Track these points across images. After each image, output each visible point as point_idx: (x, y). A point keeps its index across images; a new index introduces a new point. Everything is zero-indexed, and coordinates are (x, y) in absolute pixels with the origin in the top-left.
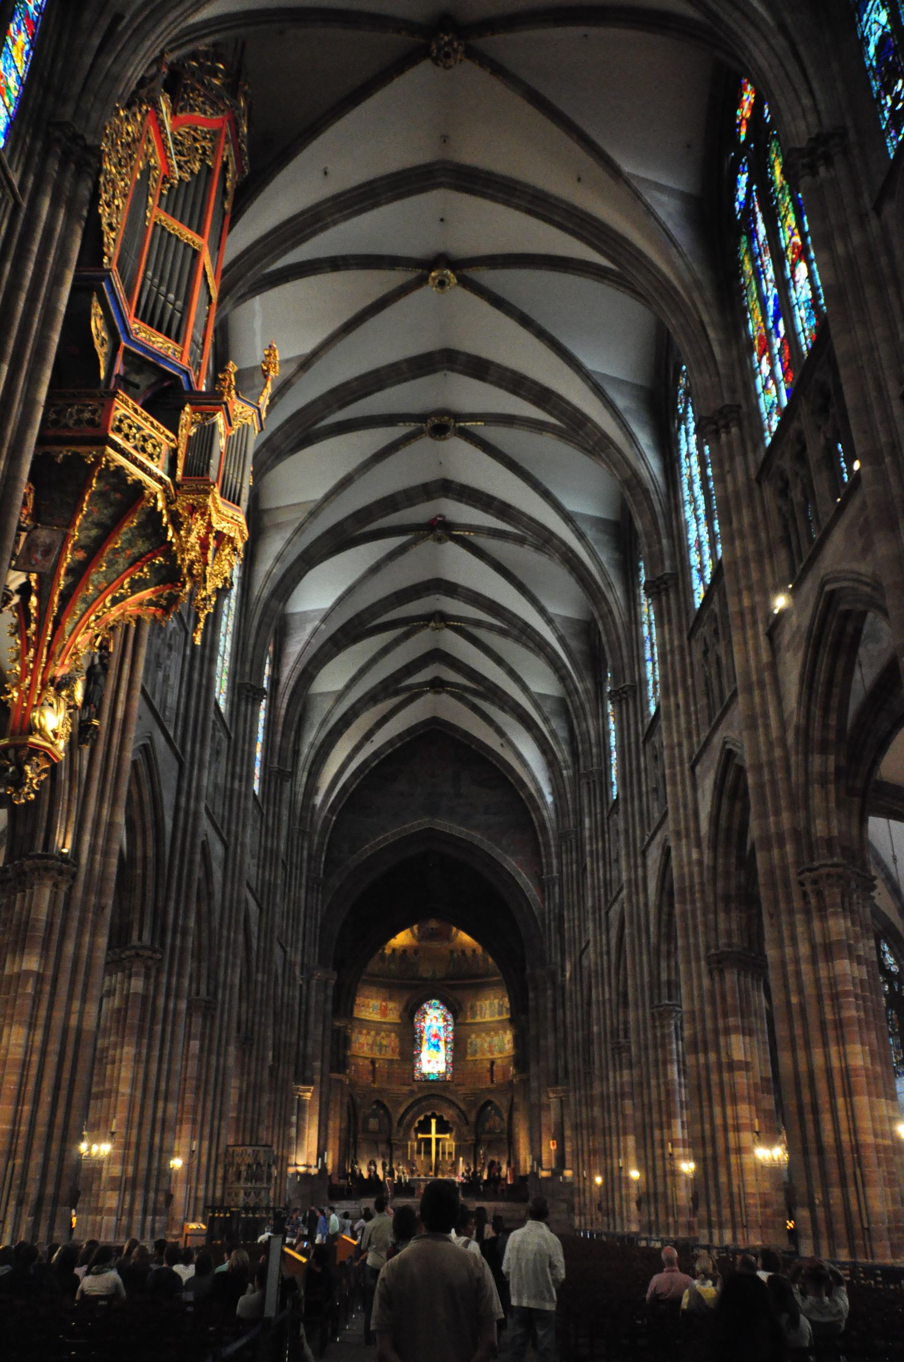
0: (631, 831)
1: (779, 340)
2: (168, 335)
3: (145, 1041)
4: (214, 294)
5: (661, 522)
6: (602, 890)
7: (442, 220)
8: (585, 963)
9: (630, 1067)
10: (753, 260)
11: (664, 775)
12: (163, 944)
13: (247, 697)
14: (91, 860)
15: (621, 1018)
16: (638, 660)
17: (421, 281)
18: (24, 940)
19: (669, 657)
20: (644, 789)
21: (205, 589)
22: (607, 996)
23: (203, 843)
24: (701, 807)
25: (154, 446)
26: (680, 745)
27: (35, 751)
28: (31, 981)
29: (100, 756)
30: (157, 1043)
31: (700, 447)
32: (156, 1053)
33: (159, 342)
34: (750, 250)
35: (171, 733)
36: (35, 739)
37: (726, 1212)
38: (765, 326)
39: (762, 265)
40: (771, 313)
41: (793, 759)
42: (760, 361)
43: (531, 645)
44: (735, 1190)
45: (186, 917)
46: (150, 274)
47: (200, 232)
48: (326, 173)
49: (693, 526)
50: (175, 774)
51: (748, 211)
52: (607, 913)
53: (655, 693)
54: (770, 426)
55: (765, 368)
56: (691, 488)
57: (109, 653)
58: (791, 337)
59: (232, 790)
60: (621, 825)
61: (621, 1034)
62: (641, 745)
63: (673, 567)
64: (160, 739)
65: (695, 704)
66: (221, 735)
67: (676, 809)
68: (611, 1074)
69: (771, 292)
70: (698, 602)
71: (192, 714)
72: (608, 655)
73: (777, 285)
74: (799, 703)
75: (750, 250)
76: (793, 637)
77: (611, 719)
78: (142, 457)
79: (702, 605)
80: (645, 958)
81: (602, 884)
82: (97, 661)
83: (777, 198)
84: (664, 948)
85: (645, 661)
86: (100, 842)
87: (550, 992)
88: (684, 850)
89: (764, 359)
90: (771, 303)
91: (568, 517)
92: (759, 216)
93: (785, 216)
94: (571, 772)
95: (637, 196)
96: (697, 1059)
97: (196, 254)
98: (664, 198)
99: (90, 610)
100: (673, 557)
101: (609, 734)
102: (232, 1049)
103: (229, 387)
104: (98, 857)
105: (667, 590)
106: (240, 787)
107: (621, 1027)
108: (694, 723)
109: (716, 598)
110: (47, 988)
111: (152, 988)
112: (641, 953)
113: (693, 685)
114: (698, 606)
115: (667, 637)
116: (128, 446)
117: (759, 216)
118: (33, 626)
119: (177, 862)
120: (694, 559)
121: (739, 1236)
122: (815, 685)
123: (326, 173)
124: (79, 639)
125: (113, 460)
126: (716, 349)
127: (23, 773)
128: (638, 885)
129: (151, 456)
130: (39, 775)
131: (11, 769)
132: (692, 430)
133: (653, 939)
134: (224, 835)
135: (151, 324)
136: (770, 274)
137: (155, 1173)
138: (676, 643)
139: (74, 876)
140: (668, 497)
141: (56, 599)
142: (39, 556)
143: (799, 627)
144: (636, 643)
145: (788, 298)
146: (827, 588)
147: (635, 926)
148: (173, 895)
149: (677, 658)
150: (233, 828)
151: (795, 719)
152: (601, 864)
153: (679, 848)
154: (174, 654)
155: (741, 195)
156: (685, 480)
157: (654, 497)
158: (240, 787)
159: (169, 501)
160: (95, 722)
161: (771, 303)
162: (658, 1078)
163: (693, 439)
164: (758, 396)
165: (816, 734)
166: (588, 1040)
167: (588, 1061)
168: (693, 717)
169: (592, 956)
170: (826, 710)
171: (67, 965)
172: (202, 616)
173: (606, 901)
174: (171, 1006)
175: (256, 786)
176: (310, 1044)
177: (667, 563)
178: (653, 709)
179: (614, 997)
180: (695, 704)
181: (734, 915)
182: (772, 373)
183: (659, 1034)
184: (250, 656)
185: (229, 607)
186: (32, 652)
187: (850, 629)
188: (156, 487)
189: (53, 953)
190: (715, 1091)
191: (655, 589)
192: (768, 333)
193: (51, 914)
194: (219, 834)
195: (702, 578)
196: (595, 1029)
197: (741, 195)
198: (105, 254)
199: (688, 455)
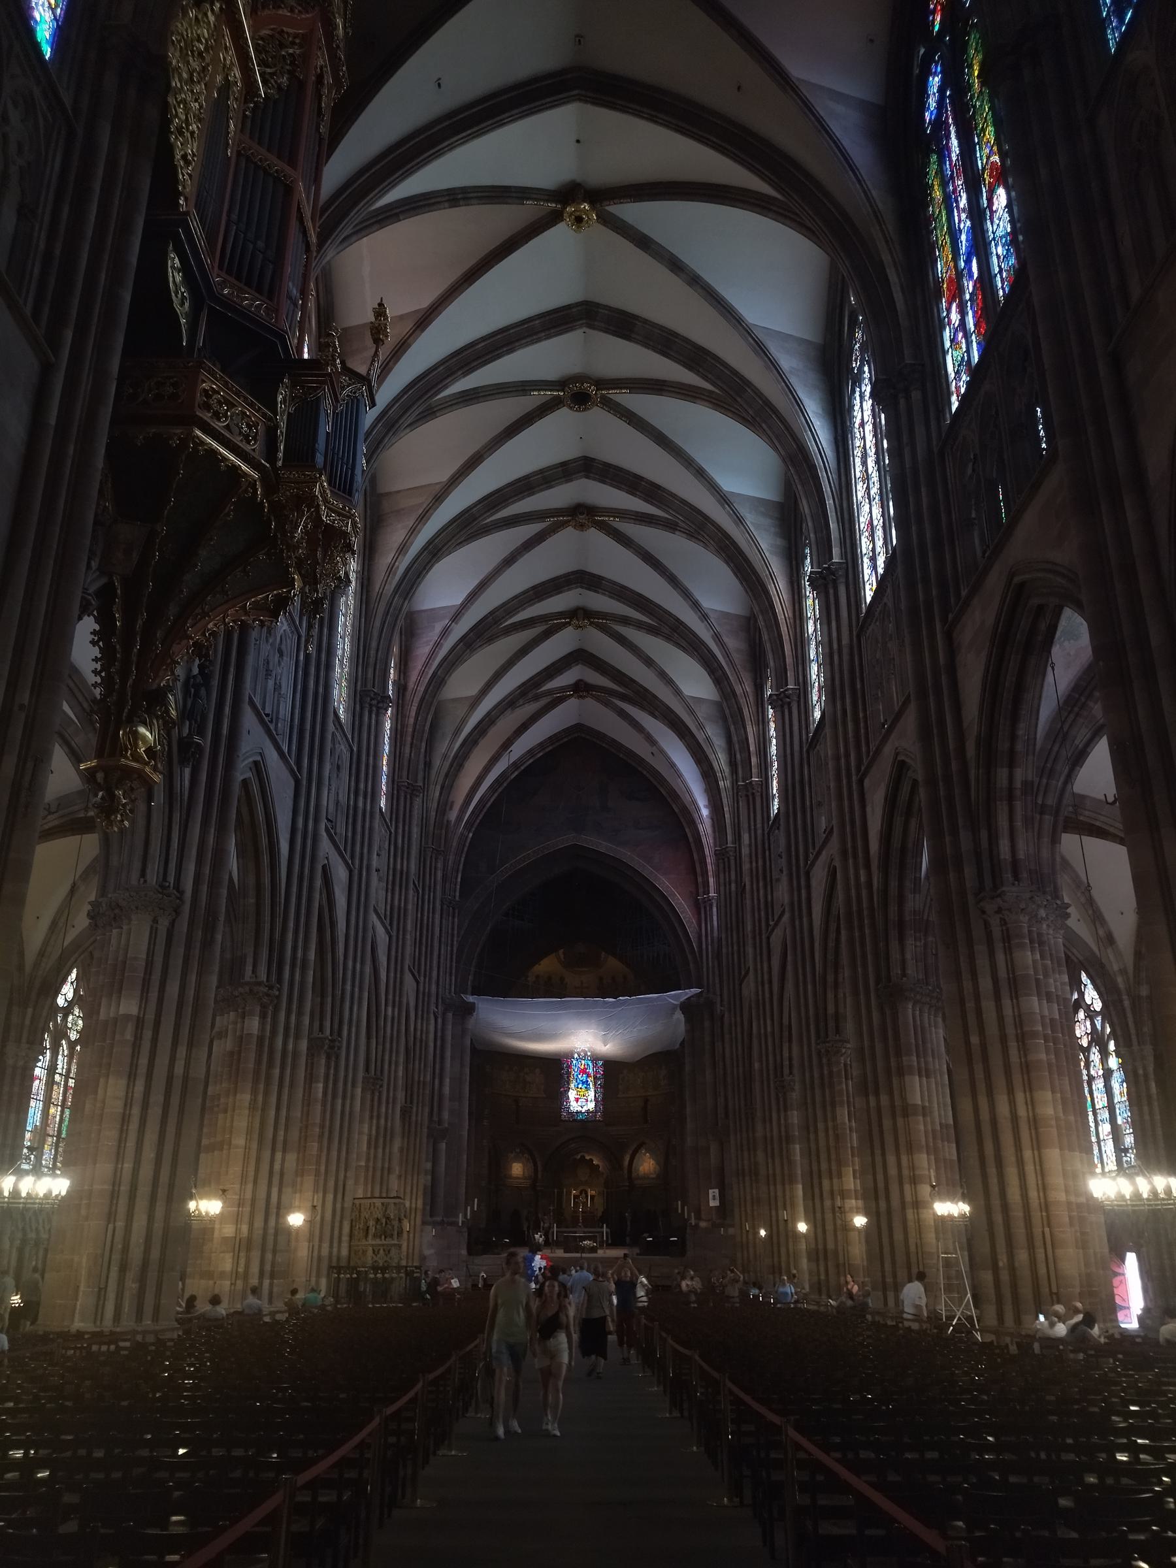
1: (971, 284)
2: (259, 290)
3: (262, 1086)
4: (314, 239)
5: (829, 502)
6: (763, 913)
7: (578, 141)
8: (745, 992)
10: (944, 185)
11: (829, 788)
12: (280, 980)
13: (371, 705)
14: (196, 891)
16: (802, 661)
17: (554, 218)
19: (836, 657)
20: (808, 803)
22: (769, 1029)
23: (324, 867)
24: (869, 823)
25: (248, 426)
26: (847, 755)
27: (128, 772)
30: (275, 1088)
31: (874, 415)
32: (273, 1100)
33: (250, 301)
34: (940, 171)
38: (956, 266)
39: (954, 191)
40: (963, 250)
41: (972, 773)
42: (949, 310)
43: (684, 644)
45: (306, 949)
46: (234, 217)
47: (292, 162)
48: (439, 85)
49: (866, 508)
50: (290, 792)
51: (939, 124)
52: (768, 938)
53: (820, 697)
54: (958, 388)
55: (955, 317)
56: (864, 463)
58: (986, 280)
60: (782, 842)
61: (786, 1071)
62: (805, 755)
63: (844, 555)
64: (272, 756)
65: (865, 710)
66: (343, 748)
69: (964, 223)
70: (869, 596)
71: (308, 726)
72: (770, 656)
73: (970, 216)
75: (940, 171)
77: (772, 725)
78: (237, 440)
80: (810, 987)
81: (762, 906)
82: (196, 671)
83: (974, 107)
84: (830, 978)
85: (811, 661)
86: (207, 870)
87: (707, 1024)
88: (852, 871)
89: (954, 306)
90: (963, 237)
91: (724, 499)
92: (952, 129)
93: (983, 130)
94: (728, 783)
95: (807, 107)
97: (289, 190)
98: (840, 109)
100: (843, 543)
101: (770, 742)
103: (333, 356)
105: (835, 582)
107: (786, 1063)
109: (889, 591)
110: (148, 1034)
111: (268, 1027)
114: (869, 599)
115: (834, 634)
116: (219, 425)
117: (952, 129)
119: (294, 889)
120: (865, 545)
123: (439, 85)
125: (203, 443)
126: (898, 296)
129: (246, 438)
131: (101, 794)
132: (867, 394)
134: (348, 857)
135: (238, 278)
136: (963, 202)
138: (845, 641)
139: (177, 911)
144: (800, 642)
145: (984, 232)
146: (1017, 580)
148: (291, 925)
149: (846, 657)
152: (761, 884)
155: (932, 103)
156: (858, 453)
157: (822, 475)
159: (270, 489)
160: (197, 739)
161: (963, 237)
162: (826, 1121)
163: (868, 405)
164: (945, 353)
169: (752, 985)
173: (768, 925)
174: (290, 1047)
175: (383, 803)
176: (447, 1081)
177: (836, 551)
178: (817, 714)
180: (865, 710)
181: (910, 942)
182: (963, 322)
184: (372, 661)
185: (347, 605)
188: (255, 475)
189: (154, 995)
191: (822, 583)
192: (959, 275)
193: (150, 953)
195: (875, 567)
196: (757, 1065)
197: (932, 103)
198: (180, 194)
199: (862, 424)
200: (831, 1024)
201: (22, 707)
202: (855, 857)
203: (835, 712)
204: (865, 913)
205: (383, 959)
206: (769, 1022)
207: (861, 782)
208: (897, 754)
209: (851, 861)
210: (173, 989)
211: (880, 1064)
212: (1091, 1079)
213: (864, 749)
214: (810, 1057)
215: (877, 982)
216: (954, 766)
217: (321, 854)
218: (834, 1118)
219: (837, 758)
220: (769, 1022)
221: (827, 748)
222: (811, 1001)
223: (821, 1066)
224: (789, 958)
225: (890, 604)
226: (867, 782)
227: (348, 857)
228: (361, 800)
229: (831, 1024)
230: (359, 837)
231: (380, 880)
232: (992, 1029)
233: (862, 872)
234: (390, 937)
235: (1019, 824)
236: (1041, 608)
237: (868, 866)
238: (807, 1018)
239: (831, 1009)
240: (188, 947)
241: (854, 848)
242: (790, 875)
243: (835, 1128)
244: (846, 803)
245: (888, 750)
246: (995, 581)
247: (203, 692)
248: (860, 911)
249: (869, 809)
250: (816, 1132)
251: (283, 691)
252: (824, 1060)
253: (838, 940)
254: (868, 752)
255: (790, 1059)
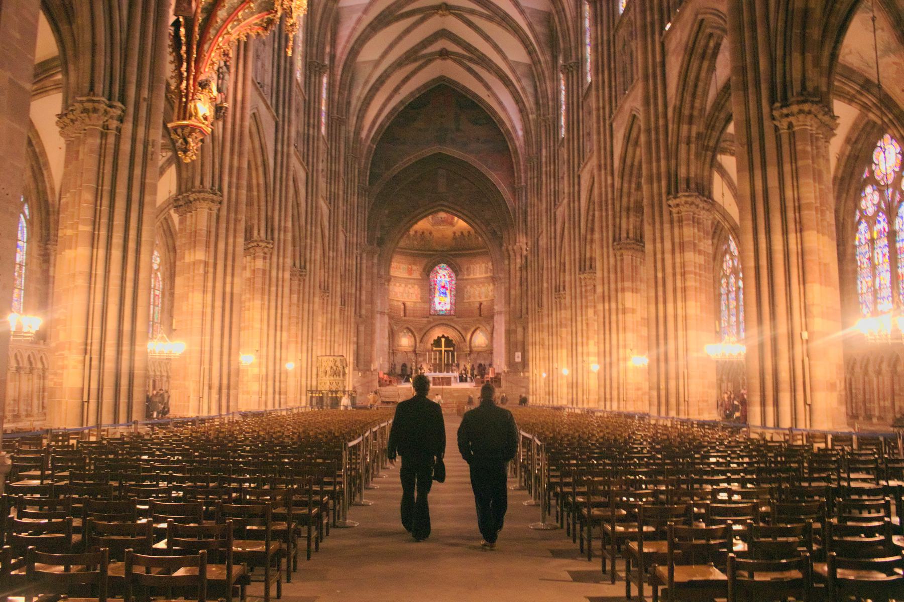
0: (571, 161)
3: (266, 297)
9: (565, 309)
12: (273, 239)
14: (229, 192)
15: (562, 279)
18: (195, 242)
21: (292, 18)
22: (553, 265)
26: (604, 108)
27: (193, 129)
28: (202, 266)
29: (229, 126)
32: (273, 304)
35: (269, 102)
36: (193, 122)
37: (615, 393)
41: (670, 126)
44: (621, 381)
57: (230, 58)
59: (308, 135)
61: (561, 288)
65: (615, 81)
66: (300, 98)
67: (599, 149)
68: (554, 313)
74: (677, 91)
76: (676, 47)
79: (624, 11)
82: (222, 64)
84: (589, 237)
86: (234, 180)
96: (604, 307)
99: (219, 34)
102: (317, 299)
104: (234, 190)
106: (314, 133)
107: (562, 284)
108: (613, 93)
109: (632, 9)
110: (211, 270)
111: (268, 265)
112: (574, 241)
113: (615, 68)
118: (184, 48)
119: (278, 186)
121: (621, 406)
122: (688, 80)
124: (213, 54)
127: (187, 142)
128: (575, 197)
130: (197, 144)
133: (583, 231)
137: (278, 372)
138: (605, 38)
139: (220, 203)
140: (577, 8)
141: (197, 29)
142: (185, 5)
143: (681, 40)
146: (700, 17)
147: (572, 222)
148: (277, 207)
149: (605, 48)
150: (311, 160)
151: (673, 102)
153: (600, 175)
154: (267, 47)
158: (314, 133)
160: (225, 105)
162: (582, 316)
165: (686, 112)
166: (541, 292)
167: (540, 305)
168: (613, 89)
170: (694, 96)
171: (221, 255)
172: (291, 36)
174: (280, 275)
176: (364, 293)
179: (558, 266)
180: (615, 81)
183: (583, 290)
186: (185, 65)
187: (712, 44)
189: (212, 249)
190: (614, 325)
193: (209, 227)
194: (302, 164)
196: (545, 285)
200: (588, 263)
201: (144, 99)
202: (606, 169)
203: (597, 82)
204: (610, 202)
205: (326, 223)
206: (553, 260)
207: (611, 125)
208: (632, 110)
209: (603, 172)
210: (221, 246)
211: (613, 286)
212: (729, 292)
213: (614, 104)
214: (575, 281)
215: (614, 240)
216: (661, 122)
217: (292, 165)
218: (586, 315)
219: (598, 109)
220: (553, 260)
221: (592, 101)
222: (577, 250)
223: (581, 286)
224: (566, 225)
225: (633, 18)
226: (614, 125)
227: (305, 164)
228: (311, 130)
229: (588, 263)
230: (311, 153)
231: (323, 176)
232: (669, 270)
233: (609, 178)
234: (330, 211)
235: (692, 157)
236: (711, 35)
237: (612, 174)
238: (575, 260)
239: (588, 255)
240: (228, 223)
241: (605, 165)
242: (569, 176)
243: (587, 319)
244: (602, 137)
245: (627, 107)
246: (688, 14)
247: (227, 77)
248: (606, 201)
249: (615, 141)
250: (576, 322)
251: (266, 67)
252: (583, 284)
253: (594, 215)
254: (616, 106)
255: (564, 282)
